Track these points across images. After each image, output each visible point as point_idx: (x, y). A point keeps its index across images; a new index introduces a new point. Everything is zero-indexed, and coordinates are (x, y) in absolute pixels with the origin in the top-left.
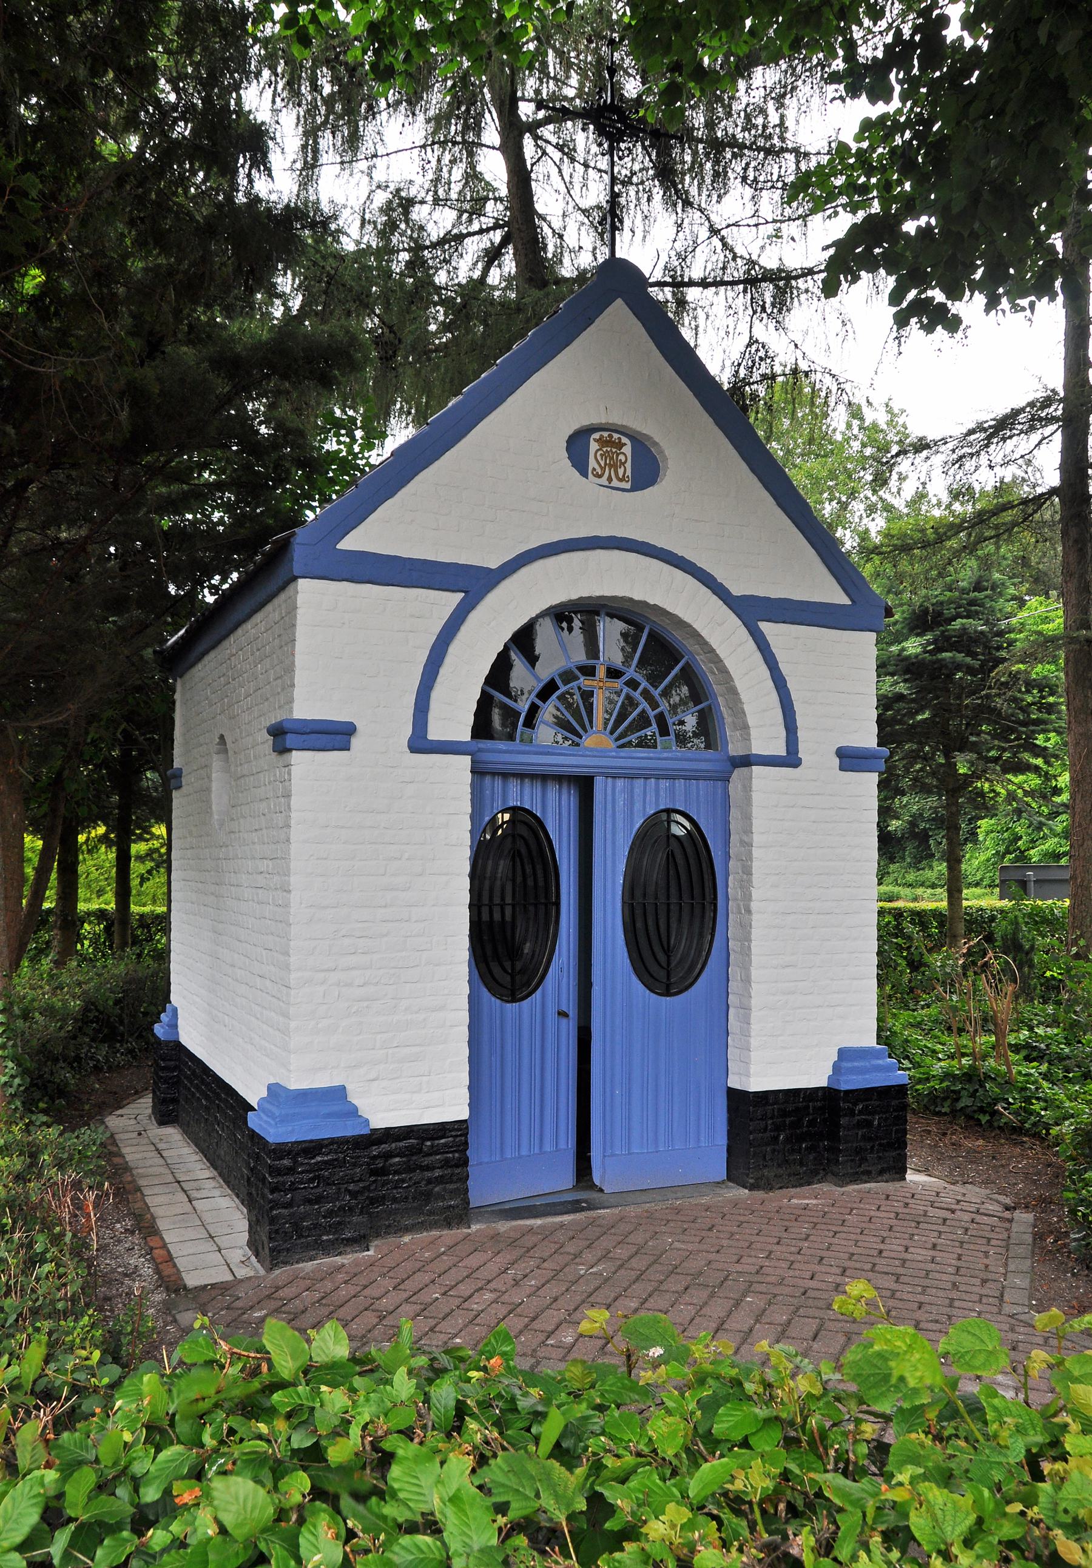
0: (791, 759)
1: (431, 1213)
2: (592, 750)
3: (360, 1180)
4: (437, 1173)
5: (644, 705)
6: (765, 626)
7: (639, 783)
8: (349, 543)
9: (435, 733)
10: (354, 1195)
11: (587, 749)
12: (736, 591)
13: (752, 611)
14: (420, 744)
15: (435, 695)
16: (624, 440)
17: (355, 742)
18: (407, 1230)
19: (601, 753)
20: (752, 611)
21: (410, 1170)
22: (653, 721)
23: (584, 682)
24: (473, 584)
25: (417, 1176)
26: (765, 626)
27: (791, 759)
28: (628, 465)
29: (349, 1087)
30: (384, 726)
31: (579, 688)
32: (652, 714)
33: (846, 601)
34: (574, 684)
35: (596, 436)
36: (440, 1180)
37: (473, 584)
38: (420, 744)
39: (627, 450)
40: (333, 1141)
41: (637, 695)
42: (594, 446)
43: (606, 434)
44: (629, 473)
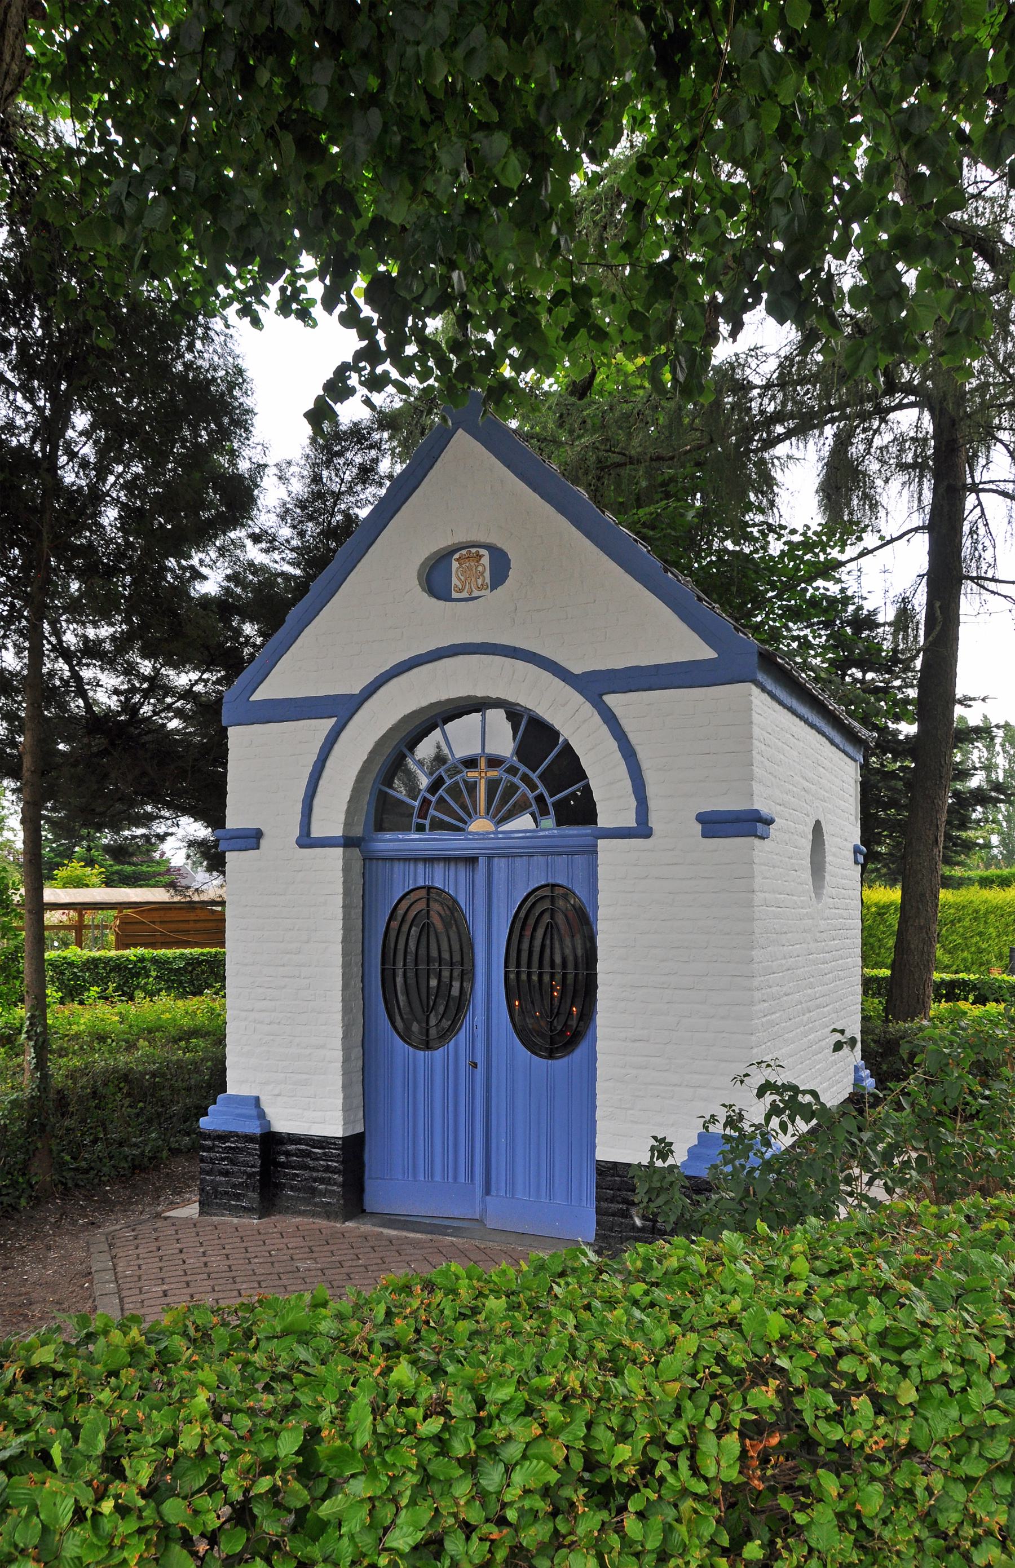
0: (642, 830)
1: (316, 1205)
2: (477, 833)
3: (253, 1166)
4: (320, 1174)
5: (523, 787)
6: (610, 699)
7: (520, 863)
8: (260, 695)
9: (315, 833)
10: (250, 1176)
11: (470, 833)
12: (577, 668)
13: (595, 687)
14: (306, 840)
15: (316, 802)
16: (483, 552)
17: (263, 842)
18: (302, 1213)
19: (483, 836)
20: (595, 687)
21: (305, 1167)
22: (533, 802)
23: (471, 775)
24: (342, 709)
25: (307, 1174)
26: (610, 699)
27: (642, 830)
28: (487, 574)
29: (262, 1098)
30: (281, 829)
31: (465, 781)
32: (531, 796)
33: (712, 654)
34: (458, 777)
35: (457, 556)
36: (322, 1180)
37: (342, 709)
38: (306, 840)
39: (486, 561)
40: (236, 1135)
41: (516, 780)
42: (455, 565)
43: (464, 552)
44: (488, 580)
